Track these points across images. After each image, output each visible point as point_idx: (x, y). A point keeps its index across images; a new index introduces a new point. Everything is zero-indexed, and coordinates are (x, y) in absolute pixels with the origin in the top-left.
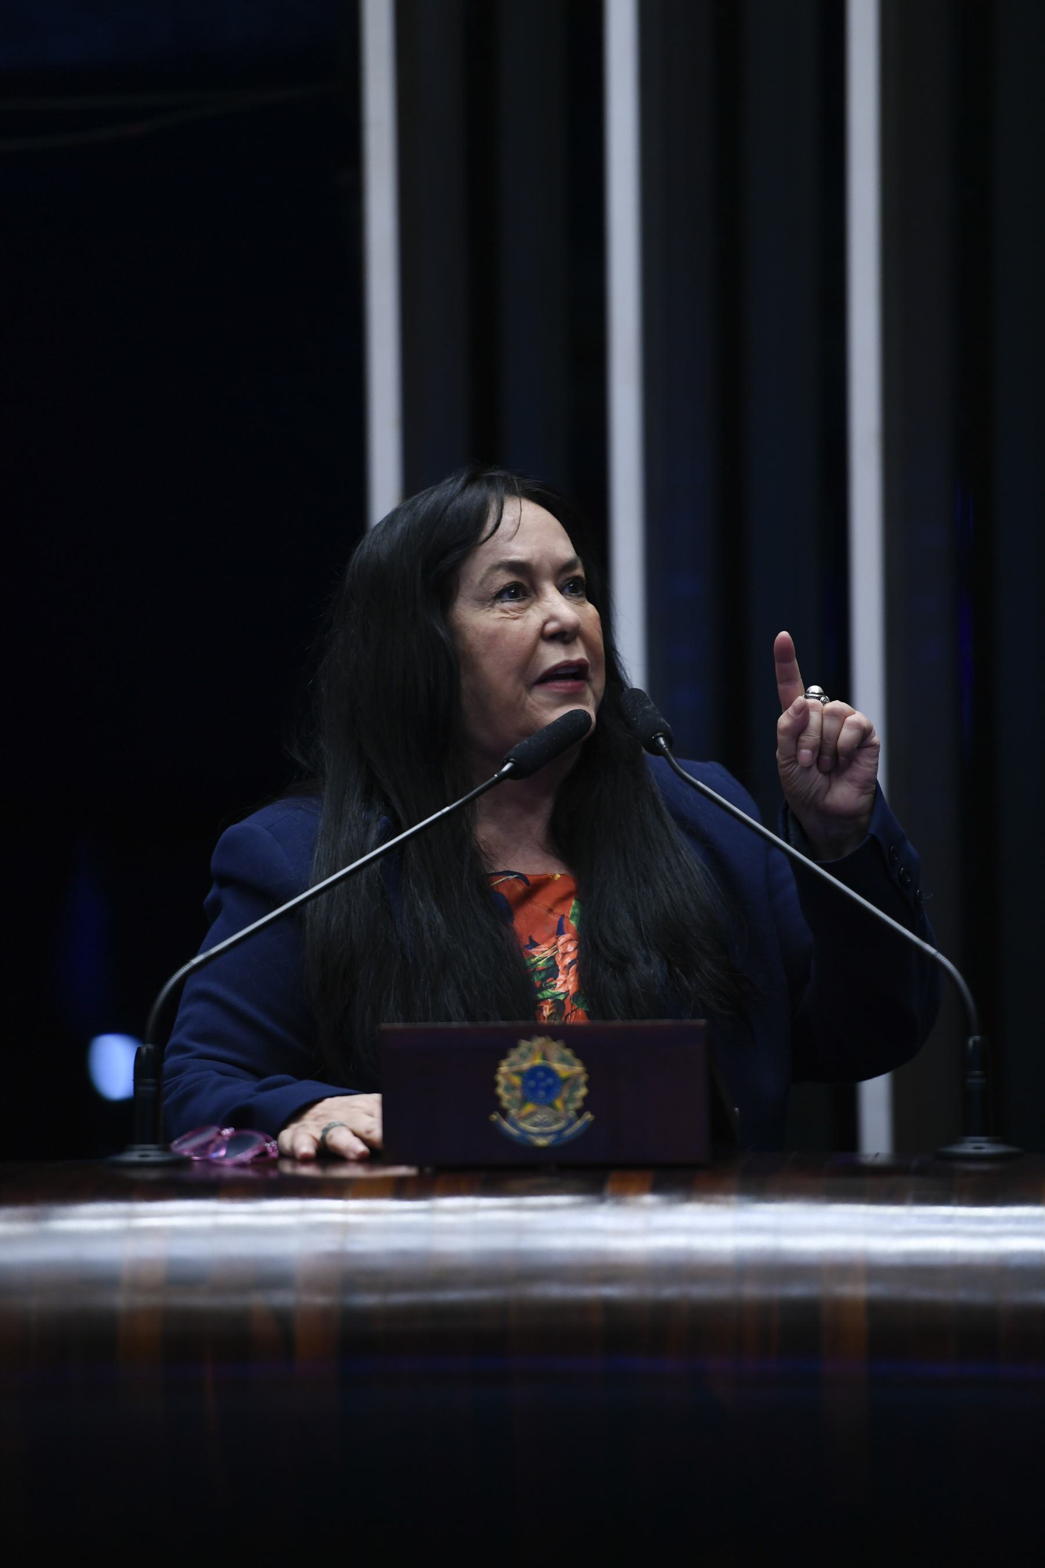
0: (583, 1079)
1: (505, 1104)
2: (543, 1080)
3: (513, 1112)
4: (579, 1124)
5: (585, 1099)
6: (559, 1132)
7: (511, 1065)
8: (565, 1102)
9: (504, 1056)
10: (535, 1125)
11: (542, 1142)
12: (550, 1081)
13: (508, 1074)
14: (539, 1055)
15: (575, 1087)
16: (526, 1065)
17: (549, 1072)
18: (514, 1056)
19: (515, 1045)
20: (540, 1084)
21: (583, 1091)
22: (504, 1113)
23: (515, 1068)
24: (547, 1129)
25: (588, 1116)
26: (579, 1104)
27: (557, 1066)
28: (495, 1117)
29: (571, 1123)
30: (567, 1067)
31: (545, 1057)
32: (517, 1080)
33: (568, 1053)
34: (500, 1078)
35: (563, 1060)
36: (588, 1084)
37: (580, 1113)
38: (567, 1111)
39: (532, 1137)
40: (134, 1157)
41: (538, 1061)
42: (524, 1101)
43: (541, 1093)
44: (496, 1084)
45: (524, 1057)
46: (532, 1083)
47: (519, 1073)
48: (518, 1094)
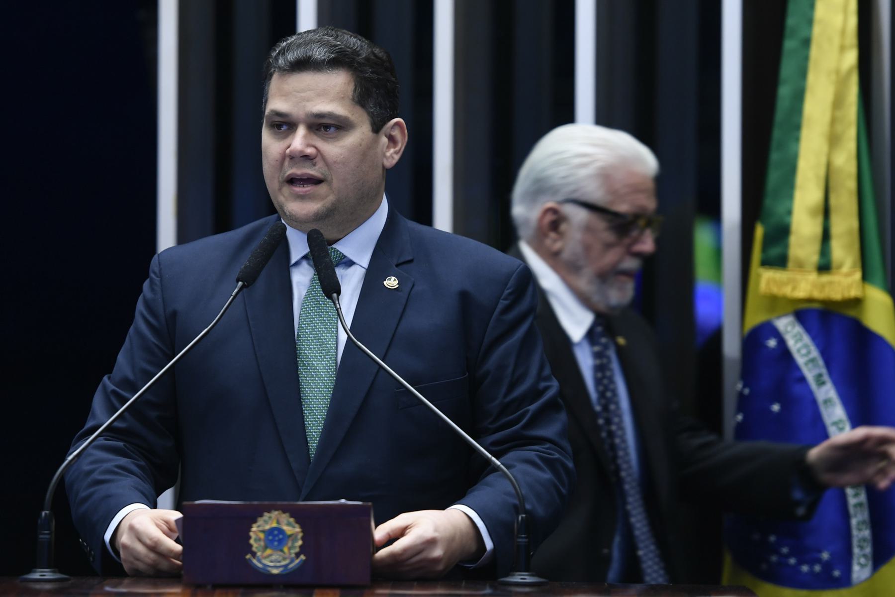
0: (300, 535)
1: (254, 549)
2: (277, 535)
3: (259, 554)
4: (297, 561)
5: (301, 547)
6: (286, 566)
7: (259, 527)
8: (290, 549)
9: (255, 521)
10: (271, 562)
11: (275, 571)
12: (281, 536)
13: (257, 532)
14: (275, 521)
15: (295, 540)
16: (267, 527)
17: (281, 531)
18: (260, 521)
19: (261, 516)
20: (276, 538)
21: (300, 543)
22: (254, 554)
23: (261, 529)
24: (278, 564)
25: (303, 557)
26: (297, 550)
27: (285, 528)
28: (248, 556)
29: (292, 561)
30: (291, 528)
31: (278, 522)
32: (262, 536)
33: (292, 520)
34: (251, 534)
35: (289, 524)
36: (303, 538)
37: (298, 555)
38: (290, 554)
39: (269, 569)
40: (36, 576)
41: (274, 525)
42: (266, 547)
43: (276, 543)
44: (250, 538)
45: (266, 522)
46: (271, 538)
47: (263, 531)
48: (262, 543)
